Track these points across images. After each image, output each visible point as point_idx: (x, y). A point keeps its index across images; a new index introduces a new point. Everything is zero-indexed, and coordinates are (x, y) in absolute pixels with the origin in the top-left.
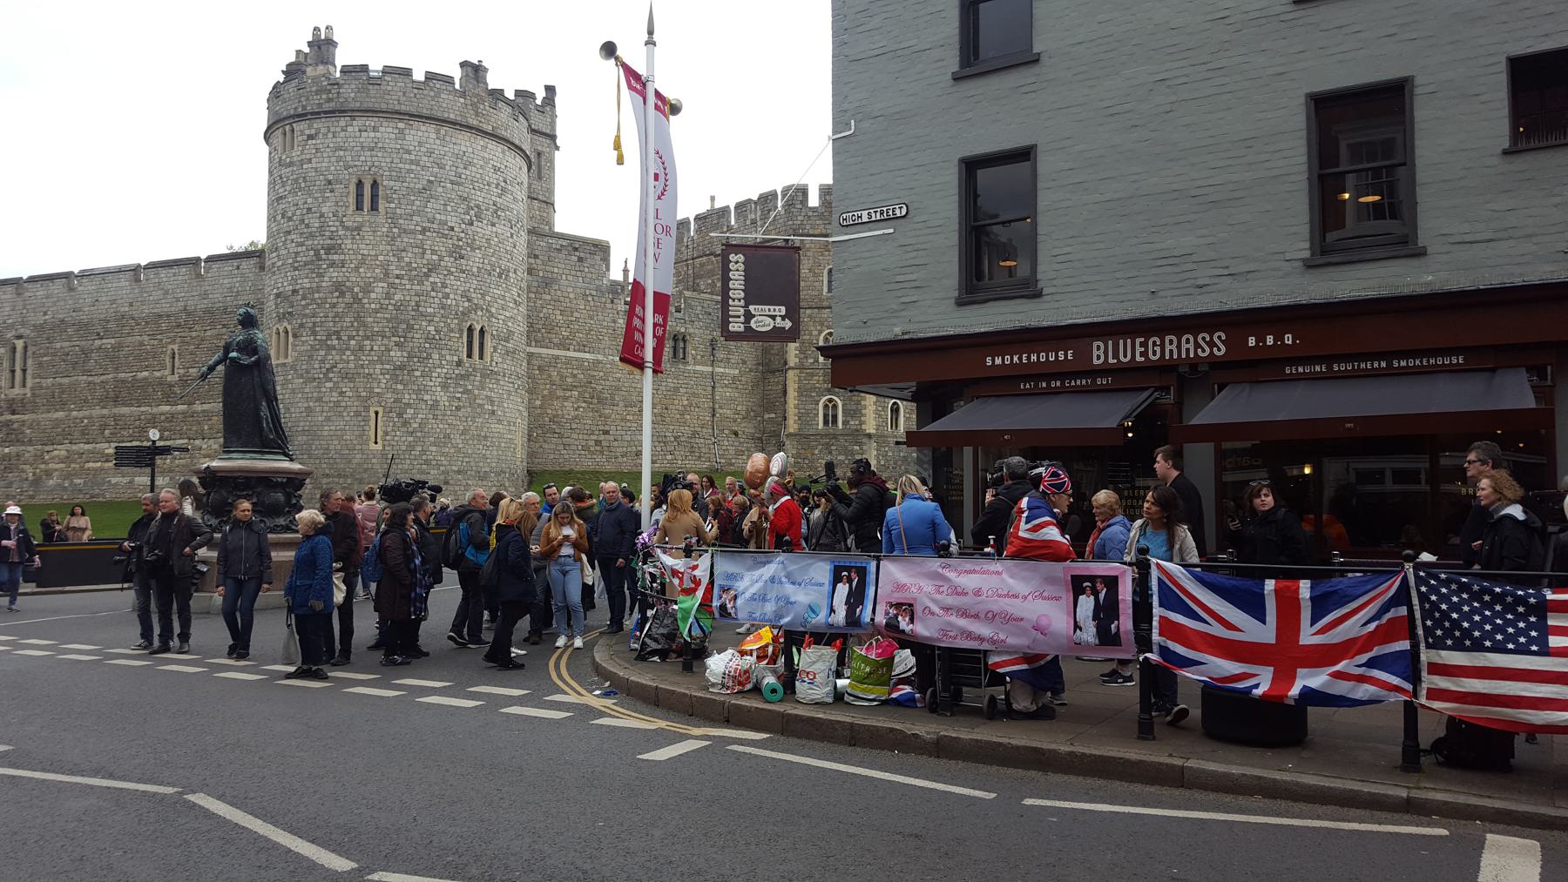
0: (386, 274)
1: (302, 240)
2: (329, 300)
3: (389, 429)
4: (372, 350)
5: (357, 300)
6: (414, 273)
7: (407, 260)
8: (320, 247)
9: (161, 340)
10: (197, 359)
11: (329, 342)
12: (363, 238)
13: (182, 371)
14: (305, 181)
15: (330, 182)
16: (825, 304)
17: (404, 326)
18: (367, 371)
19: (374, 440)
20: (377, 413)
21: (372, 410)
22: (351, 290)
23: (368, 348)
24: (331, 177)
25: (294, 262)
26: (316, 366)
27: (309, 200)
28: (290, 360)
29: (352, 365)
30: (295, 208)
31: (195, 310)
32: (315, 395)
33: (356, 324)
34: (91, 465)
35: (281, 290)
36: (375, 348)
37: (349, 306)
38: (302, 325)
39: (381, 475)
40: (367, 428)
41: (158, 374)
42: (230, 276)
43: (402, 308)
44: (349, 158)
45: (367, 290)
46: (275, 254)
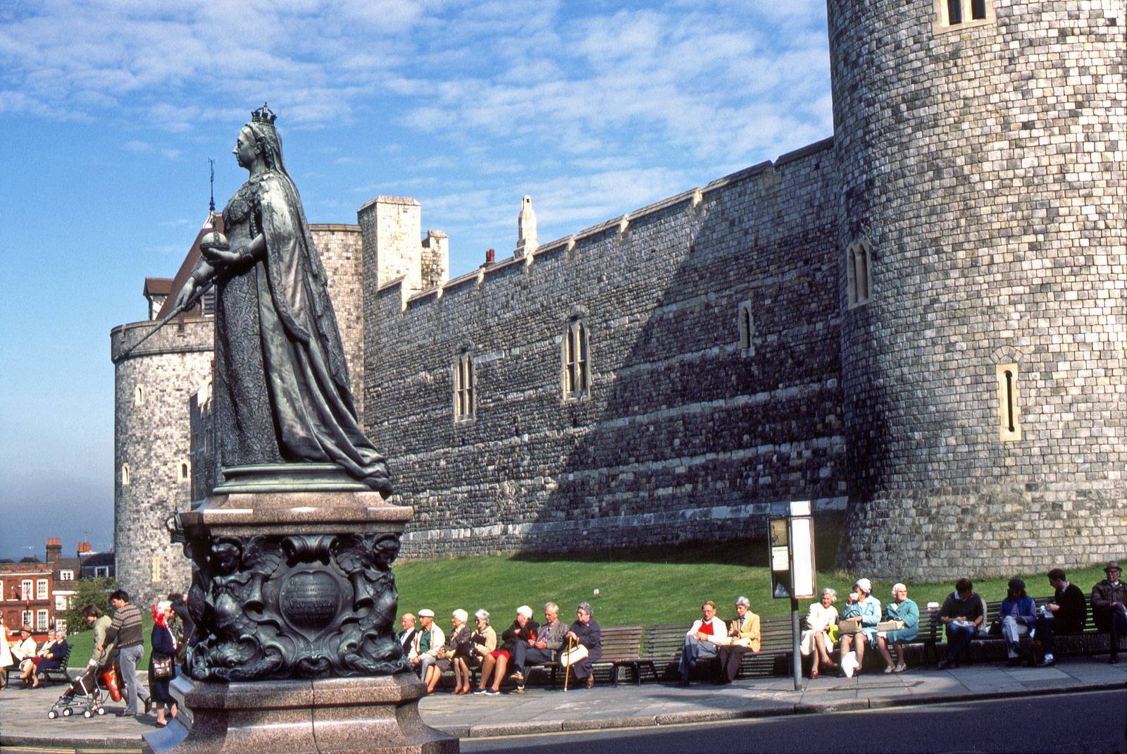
0: (1006, 125)
2: (919, 188)
3: (1031, 402)
4: (992, 263)
5: (964, 179)
6: (1053, 114)
7: (1037, 93)
9: (731, 296)
10: (776, 319)
11: (924, 260)
13: (759, 341)
17: (1042, 213)
18: (986, 302)
19: (1007, 424)
20: (1009, 375)
22: (951, 163)
23: (986, 260)
26: (908, 304)
31: (769, 244)
33: (963, 222)
34: (661, 492)
35: (852, 184)
36: (998, 259)
37: (950, 191)
39: (1022, 487)
40: (994, 403)
41: (730, 349)
42: (808, 180)
43: (1036, 181)
45: (976, 158)
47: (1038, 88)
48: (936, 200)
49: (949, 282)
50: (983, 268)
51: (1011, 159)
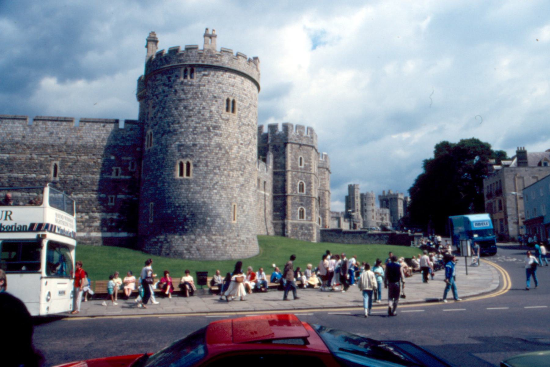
0: (238, 142)
1: (199, 121)
2: (214, 151)
5: (227, 153)
8: (210, 126)
11: (215, 171)
12: (229, 125)
14: (201, 94)
15: (215, 97)
16: (299, 170)
17: (243, 167)
20: (234, 206)
21: (233, 204)
22: (224, 147)
24: (215, 95)
25: (193, 131)
27: (204, 103)
28: (191, 177)
29: (225, 183)
30: (195, 106)
32: (208, 195)
33: (226, 164)
36: (234, 175)
37: (224, 155)
38: (199, 161)
44: (224, 88)
45: (231, 148)
46: (177, 125)
47: (244, 135)
48: (220, 155)
49: (222, 179)
50: (231, 177)
51: (238, 151)
